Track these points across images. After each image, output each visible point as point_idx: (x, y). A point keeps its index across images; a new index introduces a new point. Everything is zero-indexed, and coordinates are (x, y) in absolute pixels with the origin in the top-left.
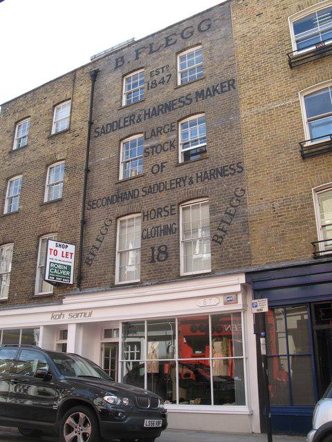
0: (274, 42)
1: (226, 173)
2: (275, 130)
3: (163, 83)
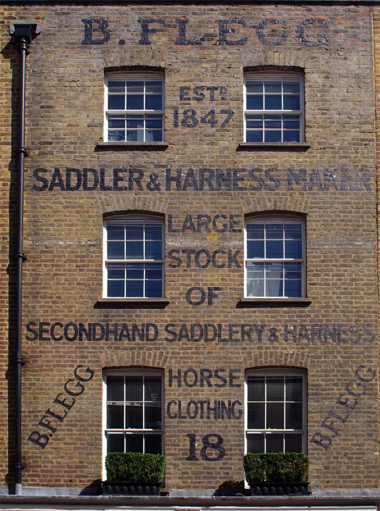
1: (343, 336)
3: (213, 123)
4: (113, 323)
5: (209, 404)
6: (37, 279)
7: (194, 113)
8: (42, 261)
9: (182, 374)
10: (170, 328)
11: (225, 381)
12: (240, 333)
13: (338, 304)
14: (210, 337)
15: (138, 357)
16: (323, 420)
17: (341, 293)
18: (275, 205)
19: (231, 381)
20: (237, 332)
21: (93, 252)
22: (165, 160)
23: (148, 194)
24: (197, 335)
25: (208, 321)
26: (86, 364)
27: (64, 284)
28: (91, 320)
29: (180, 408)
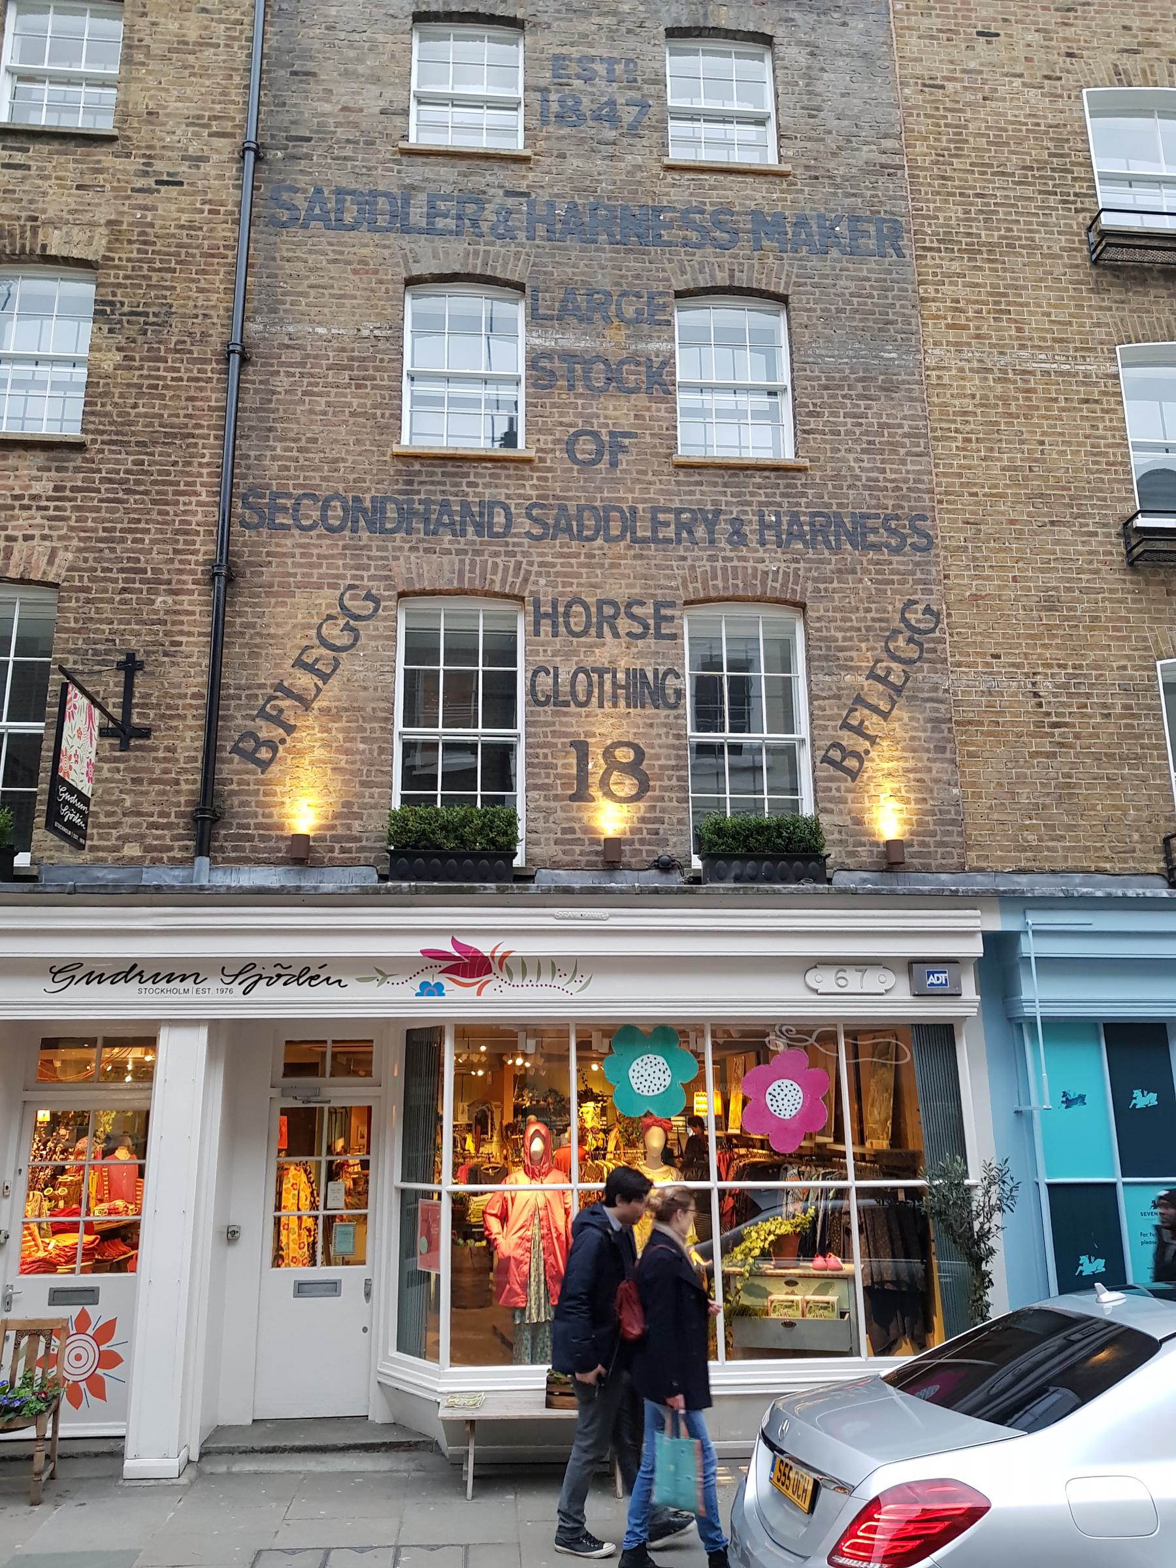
0: (1035, 152)
1: (872, 538)
2: (1042, 443)
3: (613, 119)
4: (423, 497)
5: (614, 676)
6: (270, 401)
7: (578, 102)
8: (282, 364)
9: (561, 609)
10: (534, 512)
11: (646, 627)
12: (673, 527)
13: (857, 471)
14: (615, 532)
15: (472, 571)
16: (845, 713)
17: (863, 451)
18: (732, 277)
19: (658, 627)
20: (667, 524)
21: (384, 352)
22: (525, 183)
23: (492, 244)
24: (589, 529)
25: (610, 499)
26: (365, 582)
27: (325, 413)
28: (377, 490)
29: (556, 683)
